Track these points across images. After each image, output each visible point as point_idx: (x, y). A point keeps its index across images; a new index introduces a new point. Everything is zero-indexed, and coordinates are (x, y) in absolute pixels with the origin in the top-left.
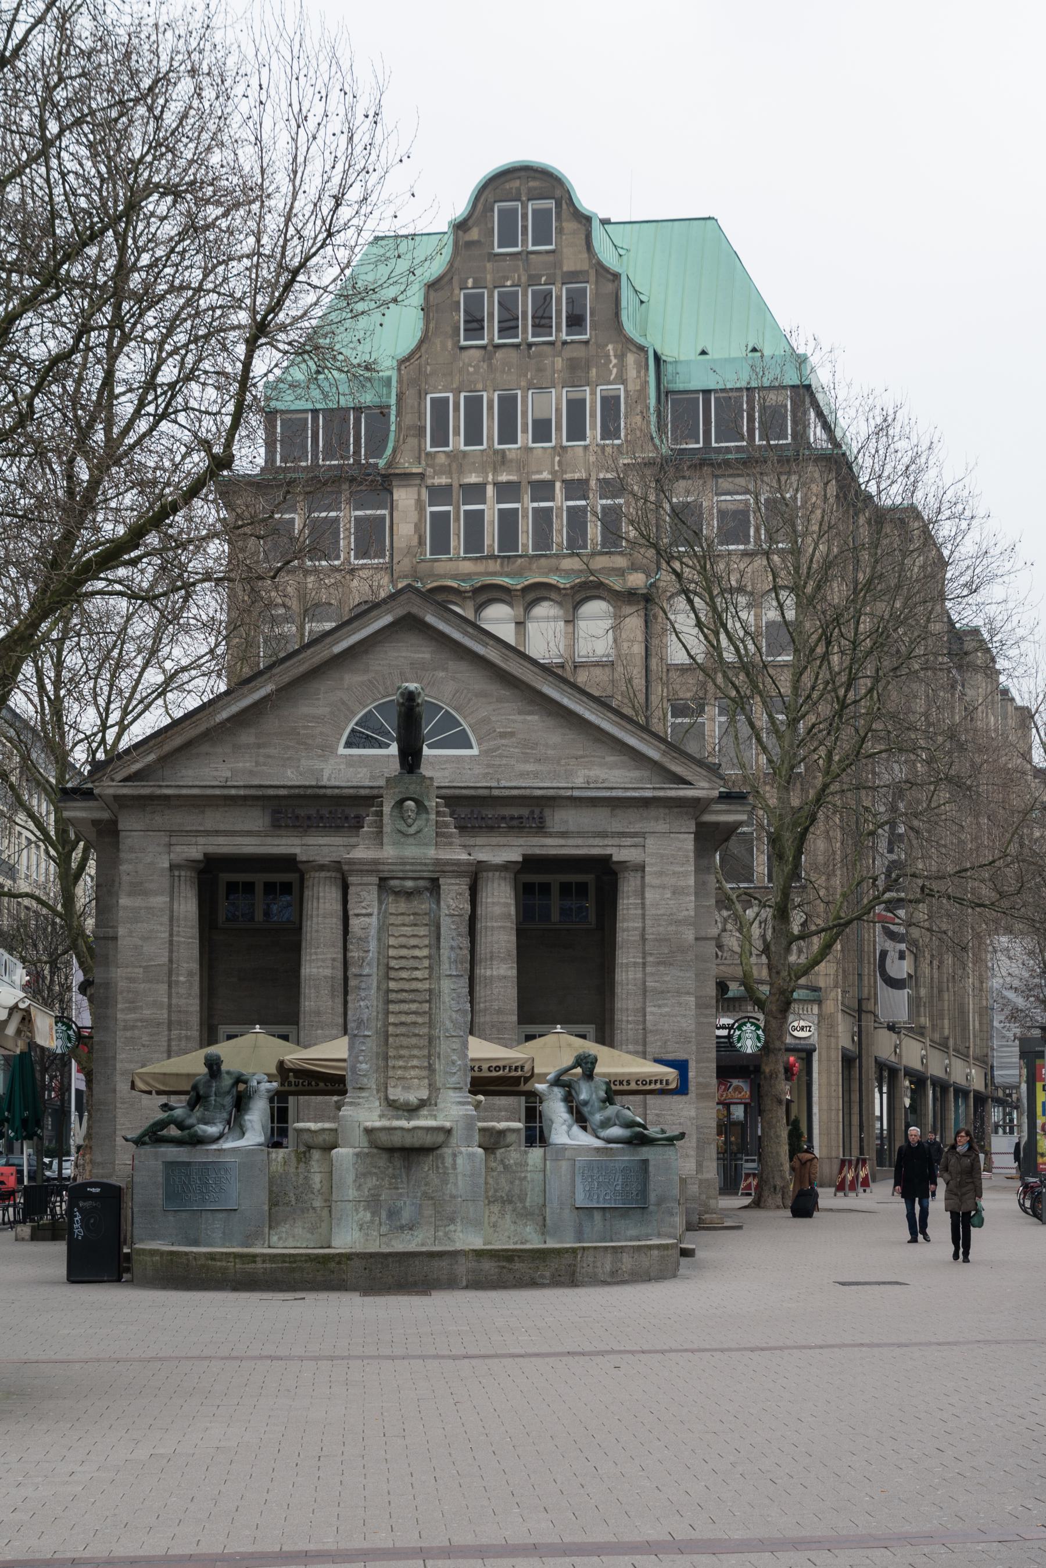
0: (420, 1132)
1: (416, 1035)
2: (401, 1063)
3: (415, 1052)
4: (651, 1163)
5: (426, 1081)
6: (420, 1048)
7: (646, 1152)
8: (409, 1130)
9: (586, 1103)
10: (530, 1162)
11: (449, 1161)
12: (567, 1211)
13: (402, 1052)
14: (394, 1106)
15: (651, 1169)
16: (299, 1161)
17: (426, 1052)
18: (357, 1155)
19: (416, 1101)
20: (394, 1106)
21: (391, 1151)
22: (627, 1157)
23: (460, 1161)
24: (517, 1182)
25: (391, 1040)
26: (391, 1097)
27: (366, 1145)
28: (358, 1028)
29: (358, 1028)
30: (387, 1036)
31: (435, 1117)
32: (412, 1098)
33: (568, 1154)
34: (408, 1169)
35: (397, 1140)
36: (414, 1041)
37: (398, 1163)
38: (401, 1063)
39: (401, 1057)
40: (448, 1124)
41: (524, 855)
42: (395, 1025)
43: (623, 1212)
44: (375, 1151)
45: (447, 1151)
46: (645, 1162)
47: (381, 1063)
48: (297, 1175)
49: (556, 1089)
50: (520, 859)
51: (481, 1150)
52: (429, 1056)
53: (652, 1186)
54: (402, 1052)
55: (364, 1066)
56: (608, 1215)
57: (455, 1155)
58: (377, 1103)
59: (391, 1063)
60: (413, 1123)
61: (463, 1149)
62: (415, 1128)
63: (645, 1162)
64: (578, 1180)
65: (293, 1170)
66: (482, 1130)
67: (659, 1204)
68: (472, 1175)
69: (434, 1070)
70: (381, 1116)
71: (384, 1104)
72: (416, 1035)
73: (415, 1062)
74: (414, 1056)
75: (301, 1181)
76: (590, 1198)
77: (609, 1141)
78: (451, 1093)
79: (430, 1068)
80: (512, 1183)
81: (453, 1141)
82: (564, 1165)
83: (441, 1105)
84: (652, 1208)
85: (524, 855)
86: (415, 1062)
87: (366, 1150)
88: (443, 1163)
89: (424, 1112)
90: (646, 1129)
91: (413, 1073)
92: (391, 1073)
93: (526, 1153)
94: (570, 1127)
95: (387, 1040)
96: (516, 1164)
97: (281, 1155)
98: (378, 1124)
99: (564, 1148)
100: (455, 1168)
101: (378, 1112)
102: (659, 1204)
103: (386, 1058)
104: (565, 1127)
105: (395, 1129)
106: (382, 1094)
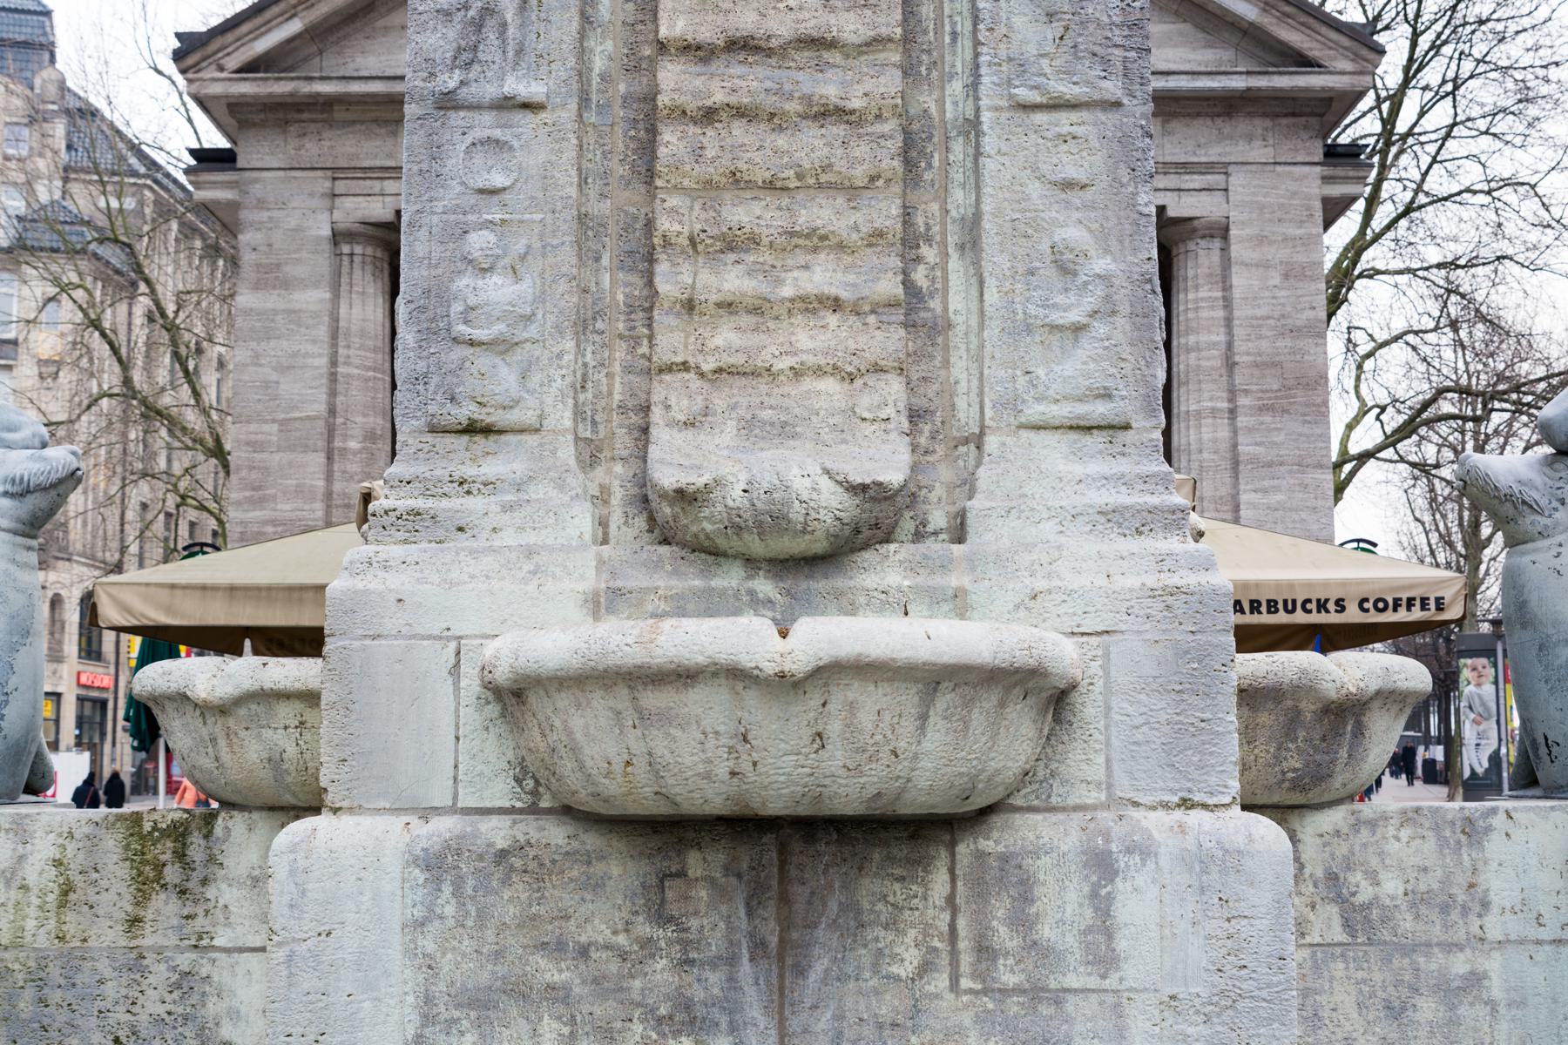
0: (871, 701)
1: (826, 113)
2: (733, 280)
3: (821, 213)
5: (894, 387)
6: (851, 191)
8: (786, 685)
10: (1500, 887)
11: (1061, 907)
13: (742, 214)
14: (680, 527)
16: (147, 881)
17: (885, 212)
18: (435, 865)
19: (832, 505)
20: (680, 527)
21: (665, 834)
23: (1138, 904)
24: (1427, 1009)
25: (671, 142)
26: (667, 477)
27: (501, 792)
28: (466, 57)
29: (466, 57)
30: (648, 117)
31: (959, 604)
32: (808, 480)
34: (784, 960)
35: (695, 759)
36: (812, 145)
37: (713, 918)
38: (733, 280)
39: (734, 244)
40: (1063, 654)
42: (693, 50)
44: (556, 834)
45: (1044, 839)
47: (616, 286)
48: (136, 964)
51: (1264, 826)
52: (910, 242)
54: (742, 214)
55: (498, 290)
57: (1102, 866)
58: (582, 521)
59: (671, 280)
60: (821, 635)
61: (1157, 823)
62: (830, 673)
65: (108, 935)
66: (1251, 696)
68: (1226, 1001)
69: (939, 329)
70: (604, 602)
71: (628, 530)
72: (826, 113)
73: (822, 276)
74: (818, 241)
75: (152, 1005)
78: (1054, 452)
79: (914, 309)
80: (1396, 1012)
81: (1085, 765)
83: (992, 531)
86: (822, 276)
87: (497, 832)
88: (1023, 922)
89: (884, 570)
91: (811, 339)
92: (671, 341)
93: (1472, 831)
95: (648, 148)
96: (1417, 900)
97: (43, 848)
98: (556, 636)
100: (1105, 960)
101: (585, 576)
103: (644, 255)
105: (684, 676)
106: (615, 476)
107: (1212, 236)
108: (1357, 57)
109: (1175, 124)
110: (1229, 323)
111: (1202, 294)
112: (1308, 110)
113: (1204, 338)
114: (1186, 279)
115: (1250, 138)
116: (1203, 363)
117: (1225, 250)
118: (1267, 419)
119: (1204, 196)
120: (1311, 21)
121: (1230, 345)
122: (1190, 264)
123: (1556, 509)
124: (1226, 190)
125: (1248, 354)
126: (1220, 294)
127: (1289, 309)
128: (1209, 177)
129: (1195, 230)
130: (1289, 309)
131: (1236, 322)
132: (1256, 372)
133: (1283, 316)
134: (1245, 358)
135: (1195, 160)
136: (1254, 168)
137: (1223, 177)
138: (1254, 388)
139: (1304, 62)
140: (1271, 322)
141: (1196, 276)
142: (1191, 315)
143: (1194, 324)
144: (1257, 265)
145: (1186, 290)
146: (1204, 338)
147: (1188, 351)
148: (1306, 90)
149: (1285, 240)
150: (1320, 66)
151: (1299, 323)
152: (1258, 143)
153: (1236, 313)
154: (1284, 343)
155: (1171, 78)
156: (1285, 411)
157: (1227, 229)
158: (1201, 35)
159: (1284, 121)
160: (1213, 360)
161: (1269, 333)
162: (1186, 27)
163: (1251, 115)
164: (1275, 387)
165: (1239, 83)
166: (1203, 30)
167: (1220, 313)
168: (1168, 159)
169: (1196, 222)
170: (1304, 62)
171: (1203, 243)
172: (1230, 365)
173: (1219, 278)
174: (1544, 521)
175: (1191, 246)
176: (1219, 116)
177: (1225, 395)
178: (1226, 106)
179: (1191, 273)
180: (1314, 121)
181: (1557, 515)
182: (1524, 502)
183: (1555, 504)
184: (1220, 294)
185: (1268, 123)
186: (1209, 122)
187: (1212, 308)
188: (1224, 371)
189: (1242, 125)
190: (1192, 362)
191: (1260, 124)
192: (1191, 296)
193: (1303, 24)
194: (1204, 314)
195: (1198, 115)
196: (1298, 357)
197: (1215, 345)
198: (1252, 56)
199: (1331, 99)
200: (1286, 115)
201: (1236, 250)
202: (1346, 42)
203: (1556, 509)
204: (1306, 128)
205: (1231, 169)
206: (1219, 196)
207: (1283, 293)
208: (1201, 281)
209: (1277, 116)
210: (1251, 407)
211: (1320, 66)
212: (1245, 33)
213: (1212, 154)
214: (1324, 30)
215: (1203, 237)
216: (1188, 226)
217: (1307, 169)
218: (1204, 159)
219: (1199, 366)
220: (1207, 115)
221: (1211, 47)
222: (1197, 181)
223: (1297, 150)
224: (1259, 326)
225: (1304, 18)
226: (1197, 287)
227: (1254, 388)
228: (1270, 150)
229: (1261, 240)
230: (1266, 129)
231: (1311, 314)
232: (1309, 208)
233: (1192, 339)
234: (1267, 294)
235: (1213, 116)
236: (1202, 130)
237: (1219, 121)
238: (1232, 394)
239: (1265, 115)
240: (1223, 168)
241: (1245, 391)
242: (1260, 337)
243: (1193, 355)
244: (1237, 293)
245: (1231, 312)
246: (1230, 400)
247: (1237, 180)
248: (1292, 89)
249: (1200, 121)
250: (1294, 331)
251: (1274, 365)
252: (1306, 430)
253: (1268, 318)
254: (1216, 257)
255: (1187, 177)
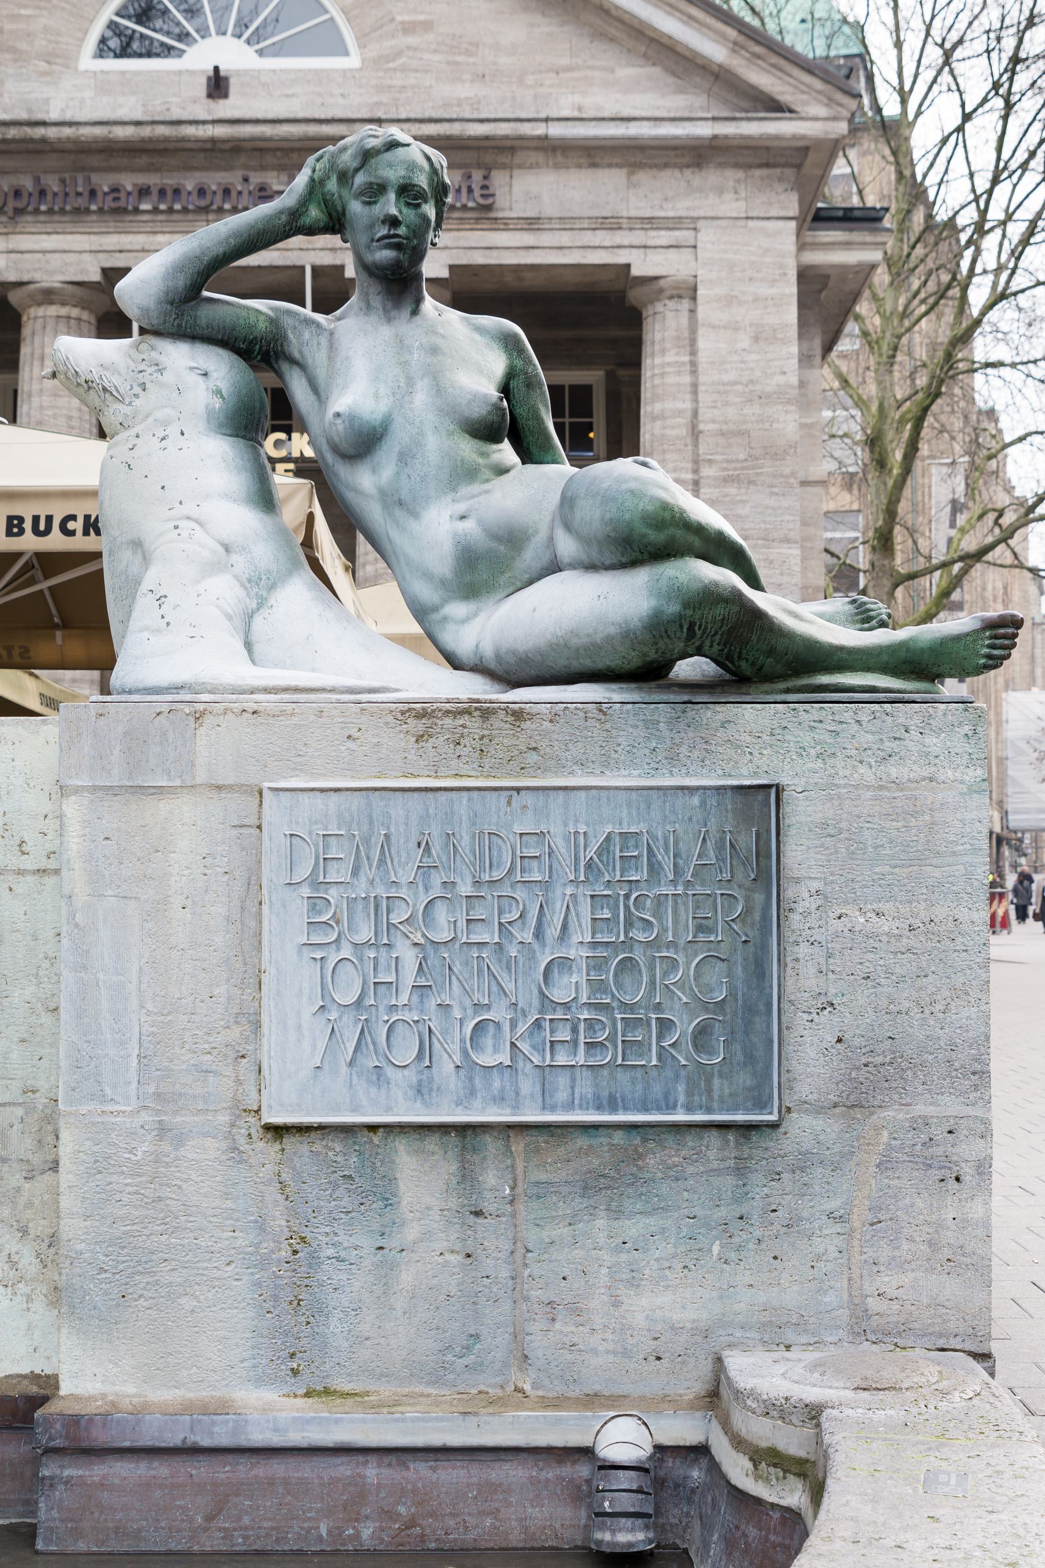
4: (801, 813)
7: (759, 737)
9: (364, 442)
12: (204, 1152)
15: (801, 855)
22: (629, 766)
33: (215, 749)
41: (452, 268)
43: (609, 1157)
46: (761, 801)
49: (180, 358)
50: (445, 274)
53: (803, 975)
56: (492, 1178)
63: (761, 801)
64: (285, 926)
67: (854, 1102)
76: (367, 1056)
77: (513, 672)
82: (188, 832)
84: (804, 1129)
85: (452, 268)
90: (755, 583)
94: (261, 588)
99: (189, 705)
102: (854, 1102)
104: (225, 590)
107: (680, 297)
108: (831, 102)
109: (643, 177)
110: (695, 388)
111: (670, 358)
112: (783, 160)
113: (669, 405)
114: (653, 343)
115: (720, 191)
116: (668, 432)
117: (692, 311)
118: (732, 490)
119: (672, 254)
120: (782, 62)
121: (695, 413)
122: (657, 327)
123: (136, 396)
124: (695, 247)
125: (714, 422)
126: (687, 359)
127: (758, 373)
128: (677, 233)
129: (661, 290)
130: (758, 373)
131: (701, 388)
132: (722, 441)
133: (752, 382)
134: (711, 427)
135: (662, 214)
136: (724, 223)
137: (692, 233)
138: (719, 457)
139: (775, 107)
140: (739, 388)
141: (663, 340)
142: (657, 381)
143: (660, 391)
144: (725, 327)
145: (653, 355)
146: (669, 405)
147: (654, 418)
148: (777, 137)
149: (755, 300)
150: (791, 111)
151: (768, 389)
152: (729, 196)
153: (702, 379)
154: (753, 410)
155: (632, 124)
156: (751, 482)
157: (695, 289)
158: (671, 80)
159: (758, 172)
160: (678, 428)
161: (737, 400)
162: (656, 71)
163: (721, 165)
164: (742, 457)
165: (704, 130)
166: (674, 74)
167: (687, 379)
168: (633, 213)
169: (662, 282)
170: (775, 107)
171: (671, 304)
172: (695, 433)
173: (687, 342)
174: (124, 409)
175: (659, 307)
176: (688, 166)
177: (689, 465)
178: (697, 155)
179: (658, 336)
180: (790, 172)
181: (137, 402)
182: (105, 389)
183: (137, 390)
184: (687, 359)
185: (741, 174)
186: (677, 173)
187: (679, 373)
188: (689, 440)
189: (712, 176)
190: (658, 431)
191: (732, 175)
192: (658, 361)
193: (774, 66)
194: (671, 379)
195: (666, 166)
196: (767, 425)
197: (680, 412)
198: (726, 102)
199: (806, 149)
200: (760, 166)
201: (702, 311)
202: (818, 84)
203: (136, 396)
204: (780, 179)
205: (700, 224)
206: (687, 254)
207: (753, 357)
208: (668, 345)
209: (750, 166)
210: (715, 478)
211: (791, 111)
212: (717, 77)
213: (680, 208)
214: (796, 72)
215: (671, 298)
216: (655, 286)
217: (781, 224)
218: (671, 214)
219: (663, 435)
220: (675, 166)
221: (682, 92)
222: (664, 237)
223: (770, 204)
224: (726, 392)
225: (774, 59)
226: (663, 352)
227: (719, 457)
228: (742, 204)
229: (729, 301)
230: (738, 181)
231: (781, 379)
232: (782, 266)
233: (658, 407)
234: (735, 358)
235: (681, 167)
236: (670, 180)
237: (688, 172)
238: (697, 463)
239: (737, 166)
240: (692, 223)
241: (710, 461)
242: (727, 404)
243: (658, 423)
244: (702, 357)
245: (697, 378)
246: (696, 471)
247: (707, 236)
248: (761, 137)
249: (666, 174)
250: (762, 397)
251: (741, 433)
252: (772, 502)
253: (736, 383)
254: (684, 319)
255: (653, 233)
